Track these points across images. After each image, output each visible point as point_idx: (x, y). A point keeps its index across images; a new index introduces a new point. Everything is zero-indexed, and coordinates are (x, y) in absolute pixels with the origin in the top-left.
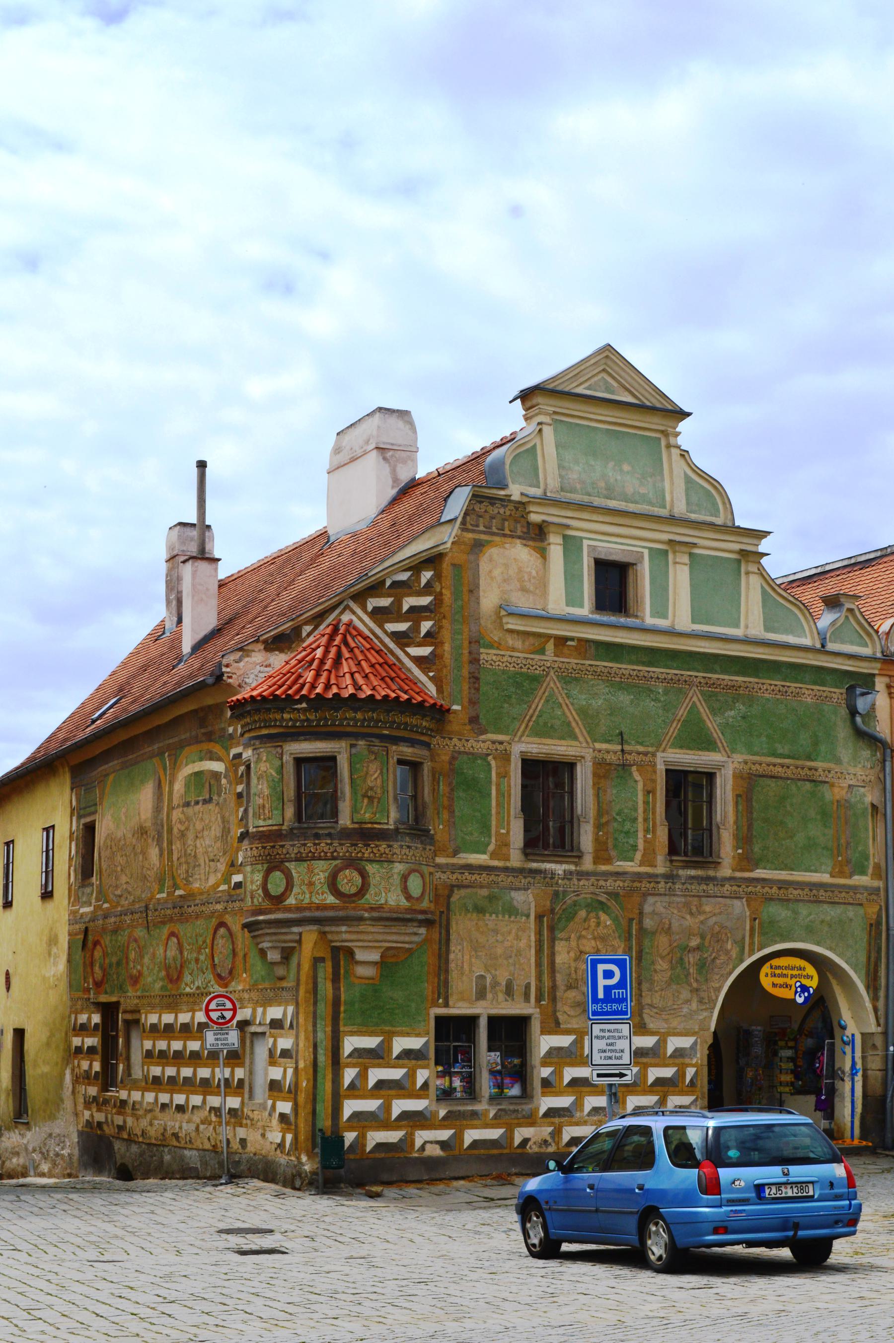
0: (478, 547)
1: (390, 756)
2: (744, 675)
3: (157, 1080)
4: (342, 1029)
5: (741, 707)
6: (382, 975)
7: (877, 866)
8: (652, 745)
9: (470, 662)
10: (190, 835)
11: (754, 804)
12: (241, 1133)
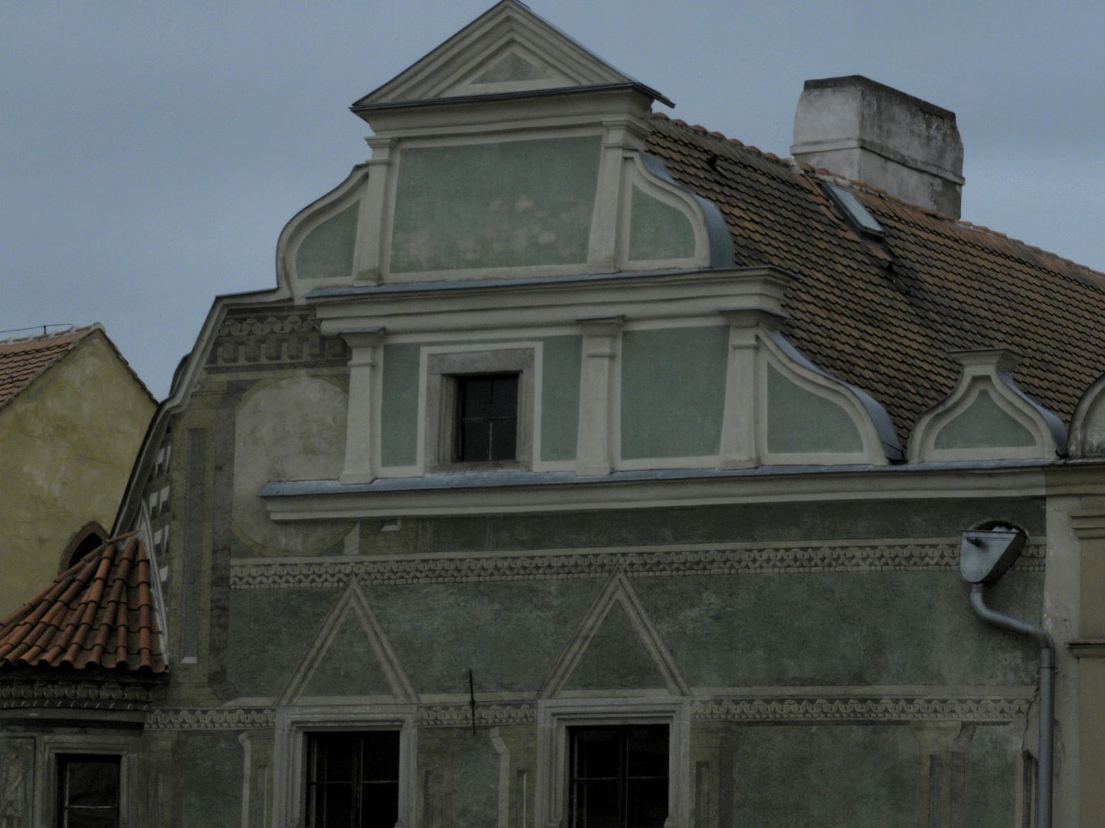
0: (235, 392)
1: (38, 752)
2: (722, 539)
5: (713, 599)
9: (214, 584)
11: (736, 777)
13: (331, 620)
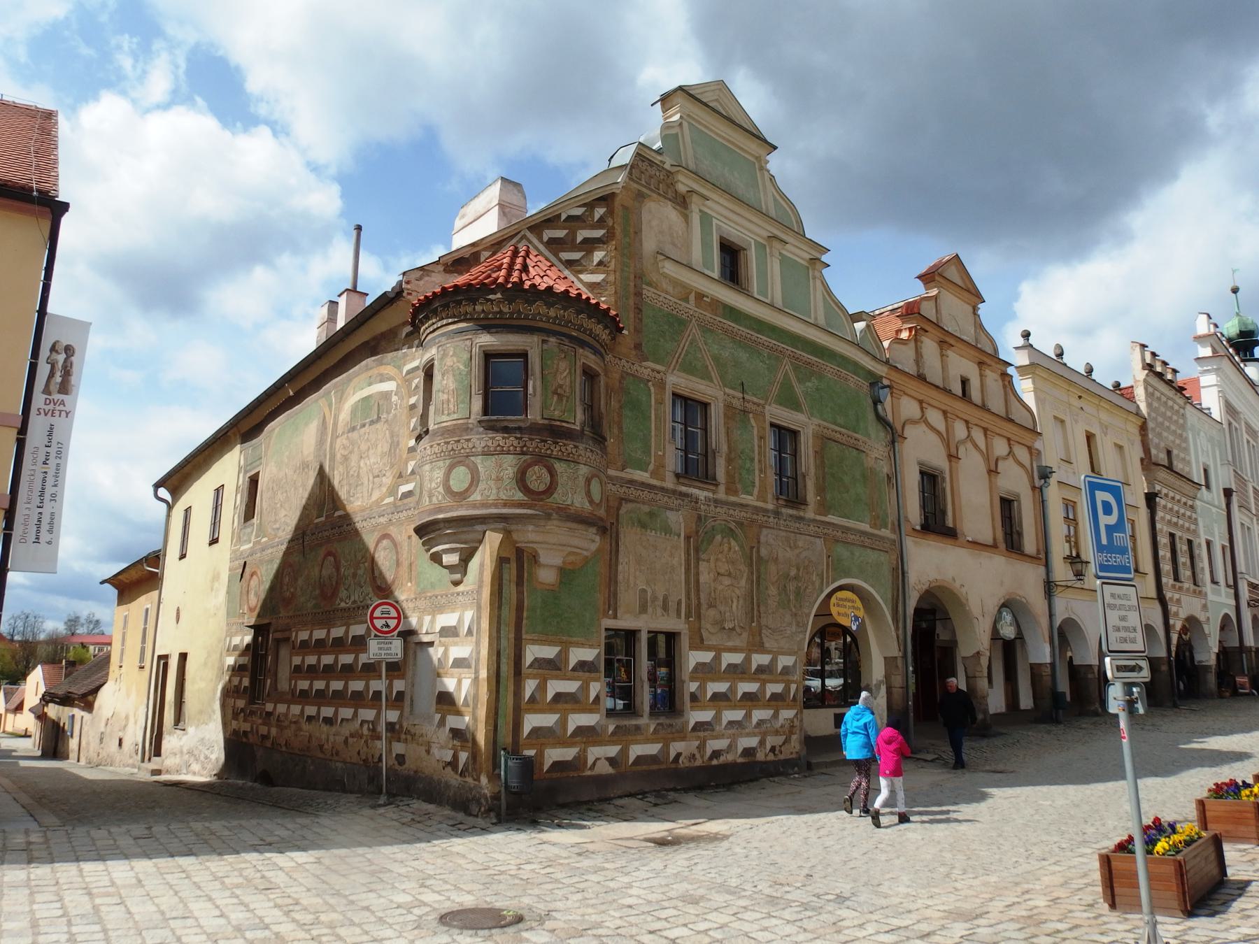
0: (640, 196)
3: (304, 693)
4: (524, 637)
6: (561, 582)
7: (893, 524)
8: (762, 399)
10: (354, 458)
11: (826, 461)
12: (398, 748)
13: (686, 336)
